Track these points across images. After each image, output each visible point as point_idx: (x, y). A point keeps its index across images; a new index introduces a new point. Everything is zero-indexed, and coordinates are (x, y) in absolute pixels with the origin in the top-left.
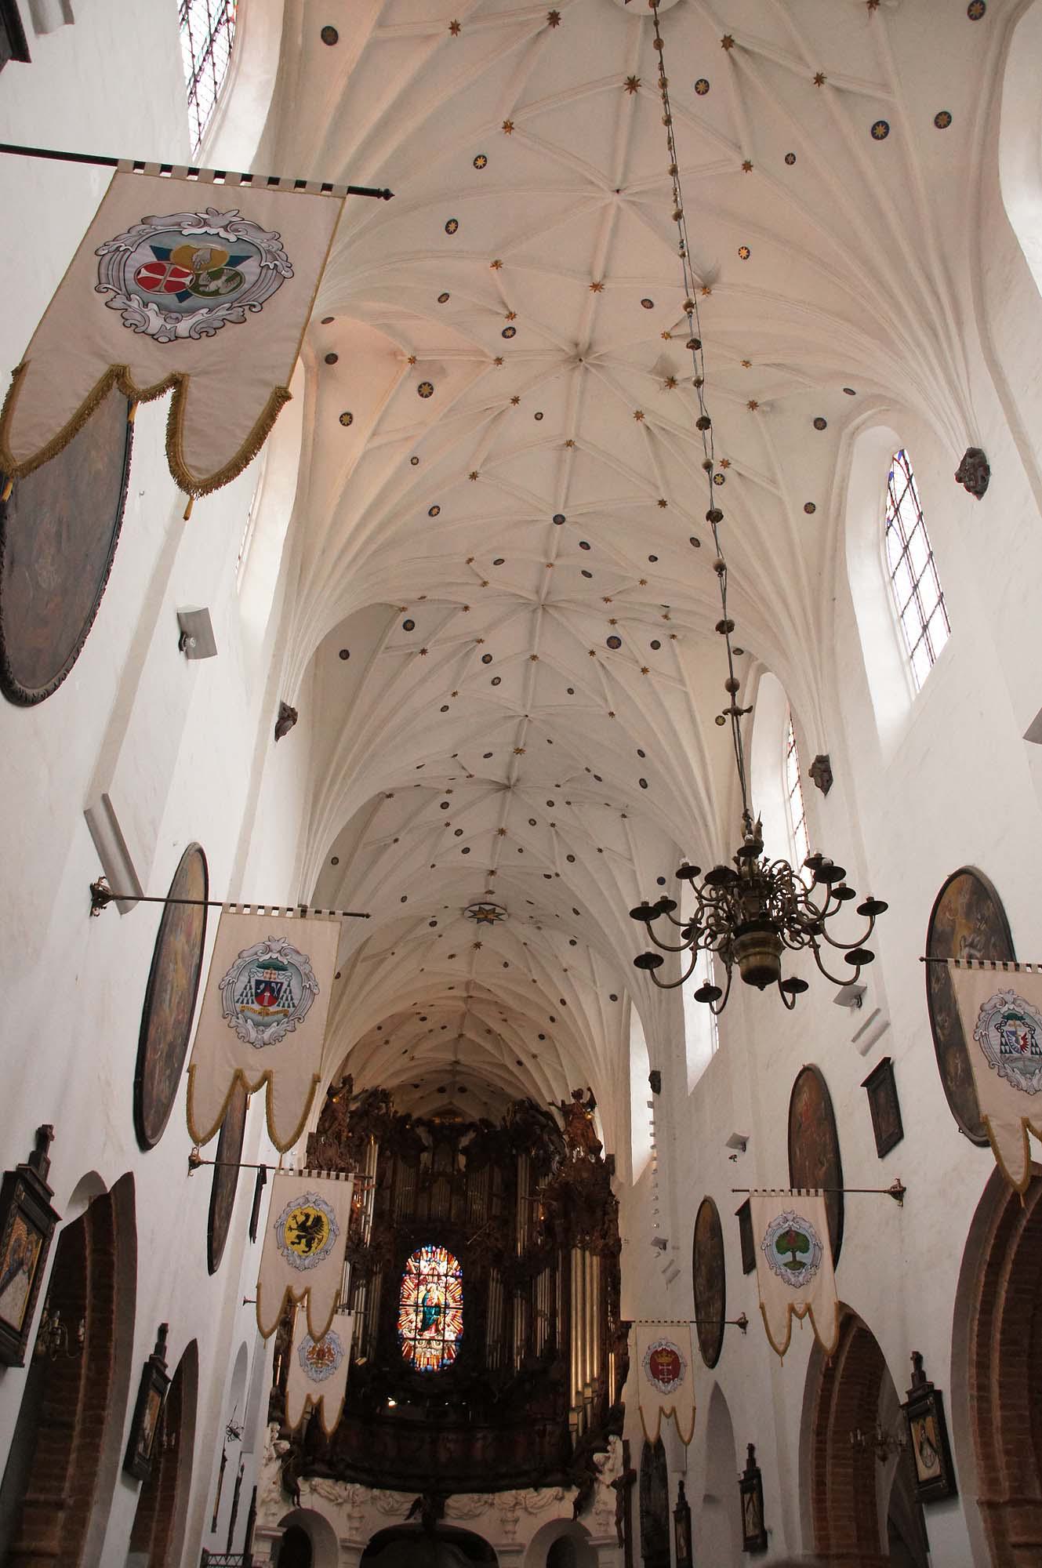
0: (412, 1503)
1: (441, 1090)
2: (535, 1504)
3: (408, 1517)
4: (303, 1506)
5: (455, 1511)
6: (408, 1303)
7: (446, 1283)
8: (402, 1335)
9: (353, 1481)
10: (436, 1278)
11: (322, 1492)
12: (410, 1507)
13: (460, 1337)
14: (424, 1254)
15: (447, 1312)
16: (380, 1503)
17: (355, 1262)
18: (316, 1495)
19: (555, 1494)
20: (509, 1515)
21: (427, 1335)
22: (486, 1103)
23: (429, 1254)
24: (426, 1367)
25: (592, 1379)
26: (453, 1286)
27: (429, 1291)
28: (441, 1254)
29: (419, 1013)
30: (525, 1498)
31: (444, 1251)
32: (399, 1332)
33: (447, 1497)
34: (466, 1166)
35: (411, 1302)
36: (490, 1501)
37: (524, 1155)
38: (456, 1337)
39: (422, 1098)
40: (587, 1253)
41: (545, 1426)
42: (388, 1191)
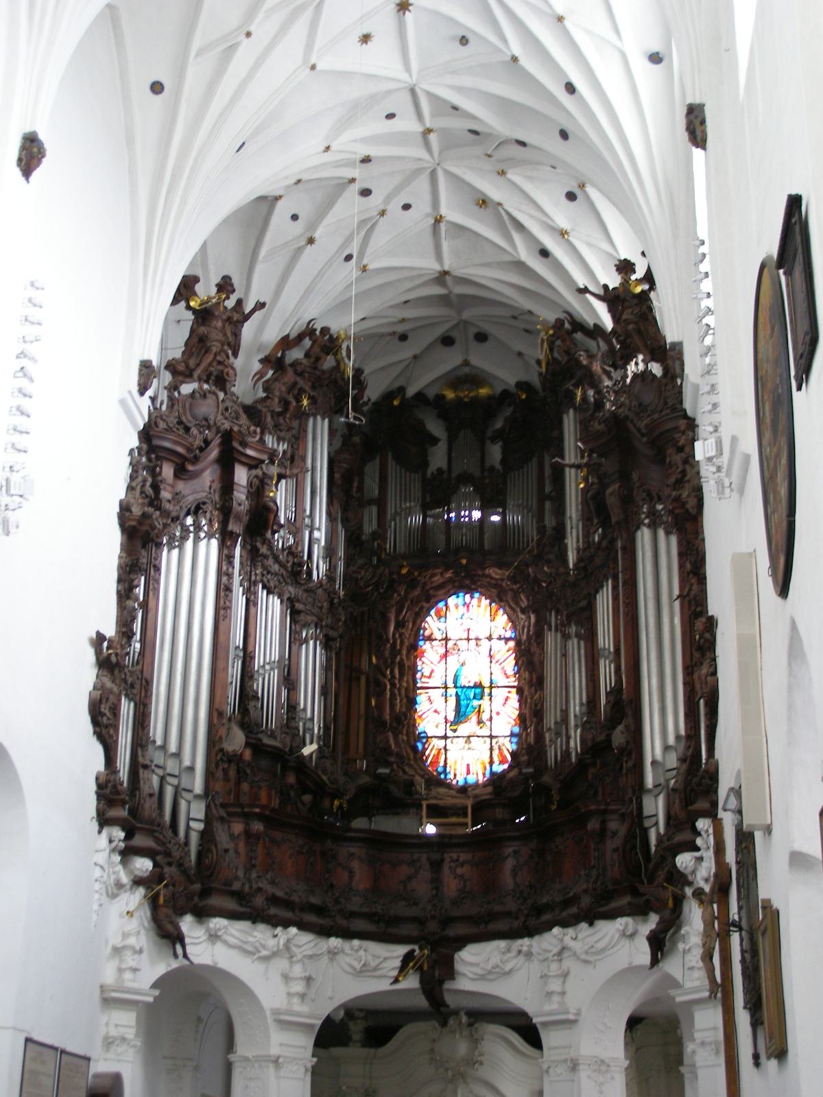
0: (401, 958)
1: (447, 341)
2: (592, 947)
3: (396, 981)
4: (196, 960)
7: (491, 650)
8: (425, 732)
9: (286, 924)
10: (473, 643)
11: (232, 940)
13: (516, 730)
16: (343, 960)
17: (289, 599)
18: (219, 947)
19: (621, 928)
20: (554, 966)
21: (464, 729)
22: (520, 354)
23: (462, 609)
24: (465, 779)
25: (678, 737)
27: (463, 664)
28: (479, 606)
29: (353, 180)
31: (485, 602)
32: (420, 729)
33: (460, 948)
34: (504, 461)
35: (436, 681)
36: (525, 949)
39: (415, 357)
41: (603, 822)
42: (374, 509)
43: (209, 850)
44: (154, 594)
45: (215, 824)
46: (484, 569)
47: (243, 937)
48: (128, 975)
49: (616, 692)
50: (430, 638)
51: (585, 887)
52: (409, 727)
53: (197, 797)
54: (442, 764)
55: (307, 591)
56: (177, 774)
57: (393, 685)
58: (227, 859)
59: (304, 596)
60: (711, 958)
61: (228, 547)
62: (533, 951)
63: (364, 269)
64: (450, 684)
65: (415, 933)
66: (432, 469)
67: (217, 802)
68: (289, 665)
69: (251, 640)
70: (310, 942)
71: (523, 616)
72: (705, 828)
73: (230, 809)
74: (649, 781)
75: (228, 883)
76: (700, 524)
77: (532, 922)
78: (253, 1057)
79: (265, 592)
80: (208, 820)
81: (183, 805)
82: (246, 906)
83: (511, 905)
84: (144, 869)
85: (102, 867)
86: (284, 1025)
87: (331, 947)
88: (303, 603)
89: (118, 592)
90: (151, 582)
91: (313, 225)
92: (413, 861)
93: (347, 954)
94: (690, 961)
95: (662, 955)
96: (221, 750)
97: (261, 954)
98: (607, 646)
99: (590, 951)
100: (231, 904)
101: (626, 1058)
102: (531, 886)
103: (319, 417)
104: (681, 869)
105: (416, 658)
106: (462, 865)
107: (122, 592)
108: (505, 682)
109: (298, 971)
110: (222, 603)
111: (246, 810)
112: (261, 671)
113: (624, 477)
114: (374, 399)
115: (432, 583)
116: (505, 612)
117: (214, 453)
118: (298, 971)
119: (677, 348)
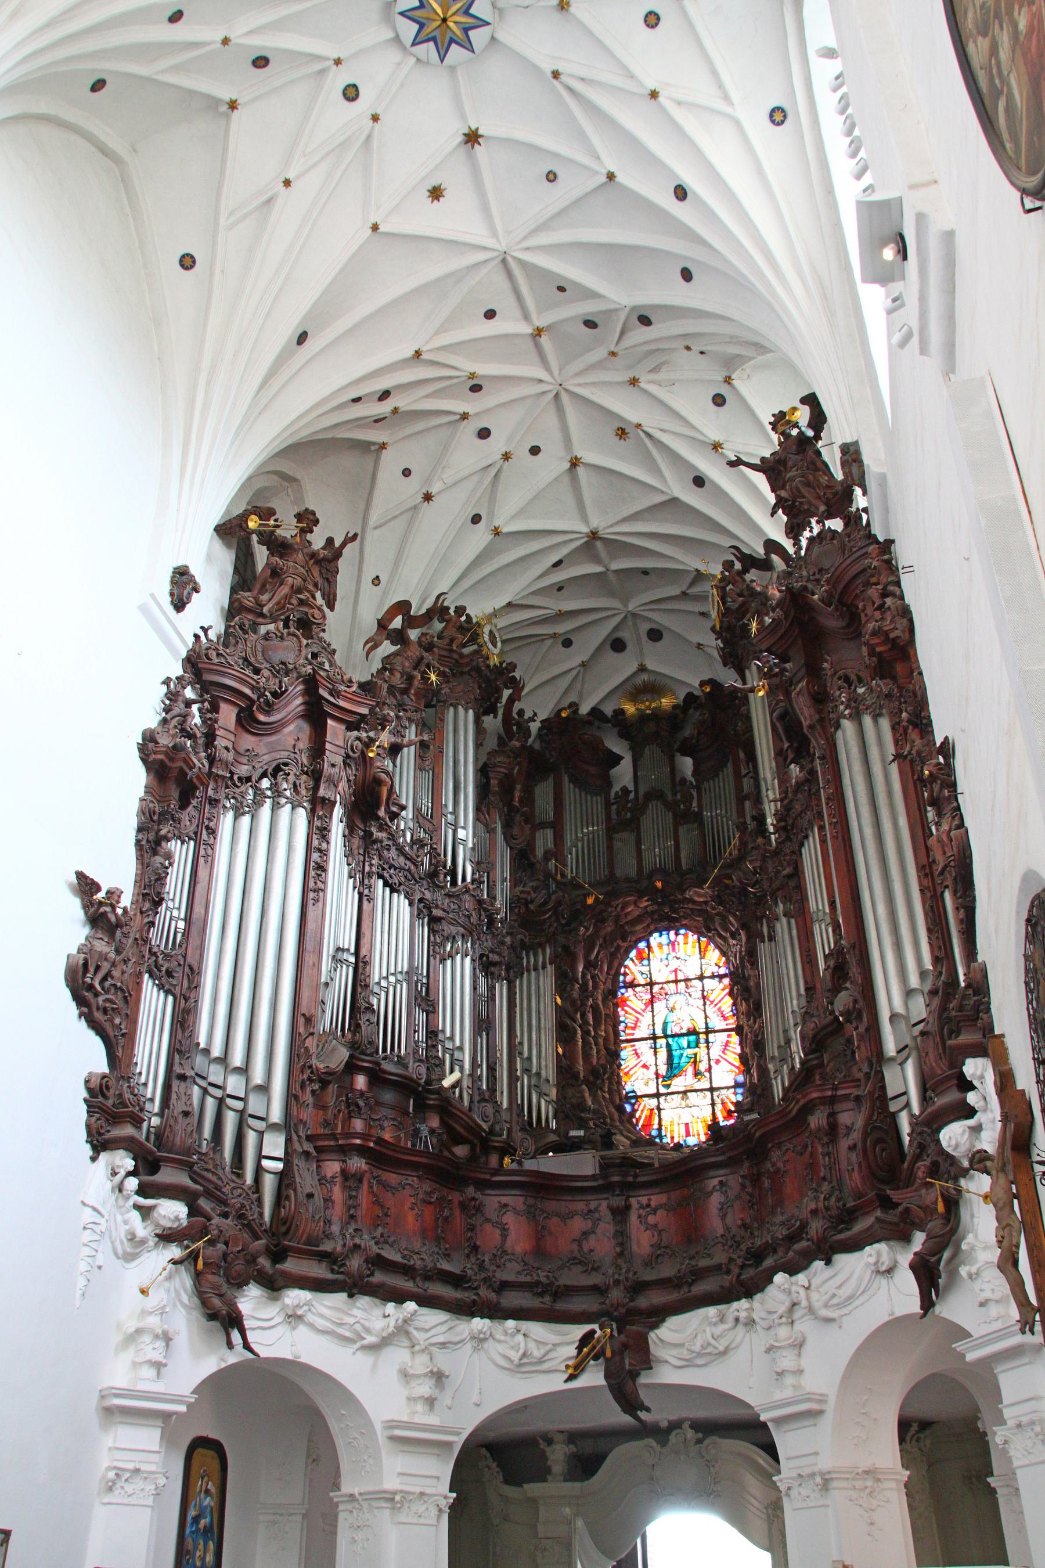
0: (577, 1344)
1: (618, 645)
2: (834, 1295)
4: (264, 1352)
5: (675, 1352)
6: (637, 1036)
7: (703, 991)
8: (634, 1091)
9: (399, 1298)
10: (681, 985)
11: (320, 1323)
13: (741, 1078)
15: (711, 1037)
18: (302, 1329)
19: (872, 1260)
20: (783, 1332)
21: (679, 1084)
22: (699, 645)
23: (666, 948)
25: (923, 974)
27: (672, 1010)
28: (686, 943)
29: (465, 416)
30: (808, 1288)
31: (692, 938)
32: (628, 1088)
33: (656, 1326)
34: (695, 773)
35: (643, 1031)
36: (743, 1315)
39: (583, 664)
40: (867, 720)
41: (832, 1115)
42: (549, 833)
43: (288, 1198)
44: (206, 862)
45: (296, 1161)
46: (684, 891)
48: (149, 1372)
49: (837, 955)
50: (632, 985)
51: (813, 1206)
52: (610, 1083)
53: (273, 1127)
54: (656, 1126)
55: (449, 895)
56: (242, 1095)
57: (586, 1033)
58: (310, 1209)
59: (447, 901)
60: (1015, 1263)
61: (320, 818)
63: (497, 532)
64: (659, 1032)
66: (616, 788)
67: (301, 1133)
68: (428, 984)
69: (365, 941)
70: (442, 1324)
71: (734, 942)
72: (979, 1073)
73: (321, 1143)
74: (890, 1047)
77: (749, 1273)
78: (361, 1494)
79: (388, 890)
80: (287, 1159)
81: (251, 1138)
82: (339, 1273)
83: (720, 1257)
84: (172, 1217)
85: (95, 1209)
87: (475, 1331)
88: (444, 910)
89: (138, 843)
90: (202, 847)
91: (428, 480)
92: (590, 1211)
93: (499, 1341)
94: (981, 1290)
95: (937, 1296)
97: (365, 1342)
98: (820, 907)
99: (831, 1303)
100: (319, 1270)
101: (905, 1466)
102: (744, 1226)
103: (461, 709)
104: (949, 1150)
105: (616, 1006)
106: (654, 1211)
107: (144, 842)
108: (721, 1025)
109: (420, 1364)
110: (311, 884)
111: (341, 1142)
112: (384, 983)
113: (813, 671)
114: (543, 715)
115: (627, 914)
116: (717, 947)
117: (296, 703)
118: (420, 1364)
119: (852, 449)
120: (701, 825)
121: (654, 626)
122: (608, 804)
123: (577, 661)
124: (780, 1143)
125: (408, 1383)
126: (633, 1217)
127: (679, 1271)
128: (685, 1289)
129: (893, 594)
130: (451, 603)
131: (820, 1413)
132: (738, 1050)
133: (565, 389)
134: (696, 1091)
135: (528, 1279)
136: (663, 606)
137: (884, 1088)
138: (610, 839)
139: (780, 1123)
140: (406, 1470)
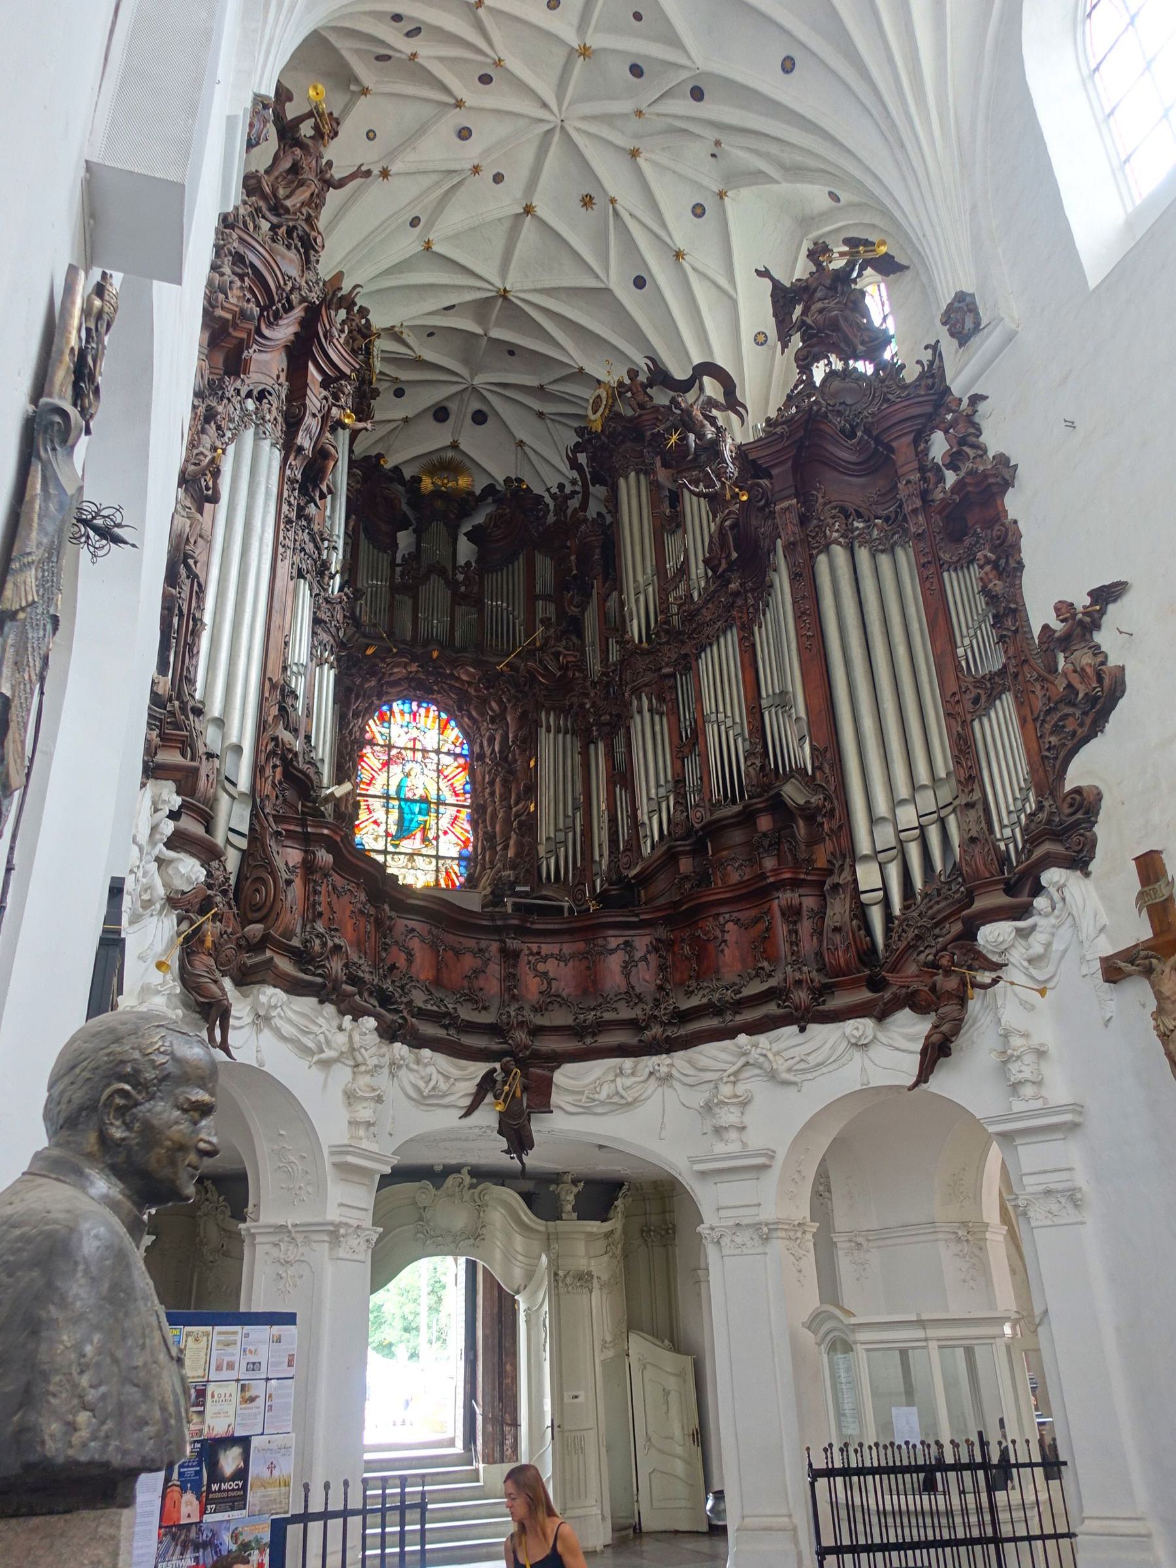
0: (478, 1080)
1: (441, 414)
4: (240, 1056)
5: (570, 1098)
7: (438, 764)
10: (419, 755)
11: (287, 1030)
12: (473, 1090)
14: (398, 715)
15: (442, 809)
18: (267, 1033)
20: (726, 1090)
21: (407, 846)
22: (521, 444)
23: (407, 716)
26: (450, 769)
27: (408, 775)
28: (427, 716)
29: (459, 104)
32: (357, 839)
35: (376, 789)
37: (633, 474)
38: (460, 853)
39: (406, 420)
40: (863, 554)
46: (456, 667)
47: (302, 1022)
53: (242, 794)
58: (289, 898)
62: (674, 1072)
63: (428, 246)
64: (392, 792)
65: (494, 1045)
74: (864, 846)
75: (288, 934)
76: (1000, 509)
77: (673, 1032)
80: (254, 836)
82: (314, 974)
83: (626, 1013)
86: (344, 1169)
91: (392, 154)
92: (480, 950)
93: (411, 1070)
96: (275, 739)
97: (323, 1056)
98: (721, 709)
99: (795, 1068)
102: (660, 988)
106: (545, 959)
110: (281, 538)
111: (309, 830)
113: (803, 494)
116: (460, 725)
119: (968, 299)
120: (481, 611)
121: (484, 408)
122: (393, 564)
123: (402, 415)
124: (718, 914)
125: (350, 1105)
126: (524, 959)
127: (585, 1021)
128: (589, 1040)
129: (975, 446)
130: (360, 302)
131: (765, 1167)
132: (468, 827)
133: (562, 128)
134: (422, 855)
135: (435, 1008)
136: (507, 393)
137: (855, 881)
138: (392, 597)
139: (728, 895)
140: (344, 1202)
